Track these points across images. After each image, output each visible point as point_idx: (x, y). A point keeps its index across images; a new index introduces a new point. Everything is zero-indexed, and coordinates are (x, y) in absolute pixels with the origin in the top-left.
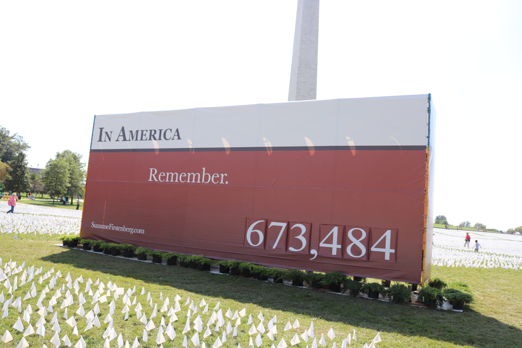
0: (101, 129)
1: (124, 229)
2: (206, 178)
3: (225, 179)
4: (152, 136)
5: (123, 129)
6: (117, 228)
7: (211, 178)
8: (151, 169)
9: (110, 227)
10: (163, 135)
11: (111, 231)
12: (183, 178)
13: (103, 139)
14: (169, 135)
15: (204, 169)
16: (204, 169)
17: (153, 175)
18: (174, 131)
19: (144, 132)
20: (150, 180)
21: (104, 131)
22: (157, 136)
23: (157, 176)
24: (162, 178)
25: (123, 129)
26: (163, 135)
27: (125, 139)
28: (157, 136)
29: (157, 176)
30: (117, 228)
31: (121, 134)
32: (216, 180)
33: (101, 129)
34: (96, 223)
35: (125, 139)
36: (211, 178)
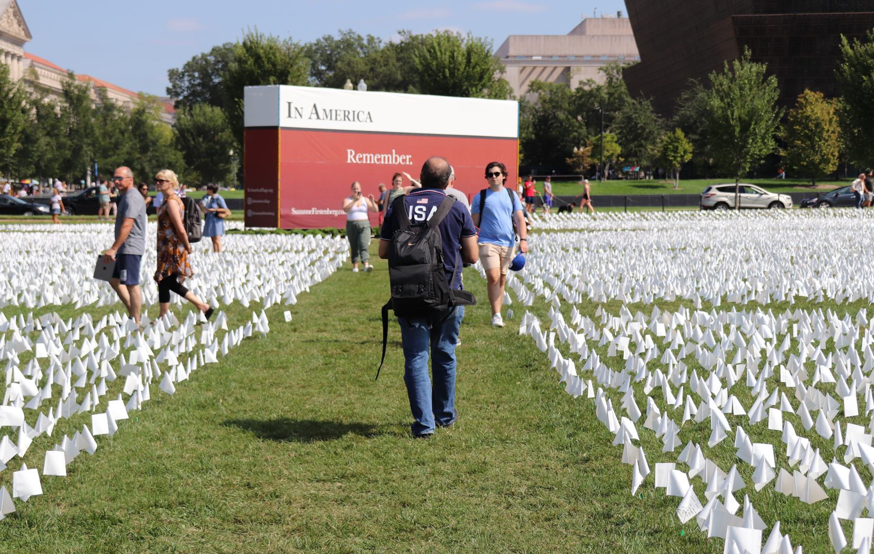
0: (289, 103)
1: (328, 212)
2: (396, 158)
3: (410, 160)
4: (346, 117)
5: (315, 106)
6: (321, 212)
7: (400, 160)
8: (349, 151)
9: (314, 211)
10: (357, 116)
11: (315, 215)
12: (379, 160)
13: (292, 114)
14: (361, 117)
15: (394, 151)
16: (394, 151)
17: (352, 157)
18: (366, 113)
19: (338, 112)
20: (349, 161)
21: (292, 106)
22: (351, 116)
23: (355, 157)
24: (361, 159)
25: (315, 106)
26: (357, 116)
27: (318, 118)
28: (351, 116)
29: (355, 157)
30: (321, 212)
31: (314, 111)
32: (404, 160)
33: (289, 103)
34: (297, 209)
35: (318, 118)
36: (400, 160)
